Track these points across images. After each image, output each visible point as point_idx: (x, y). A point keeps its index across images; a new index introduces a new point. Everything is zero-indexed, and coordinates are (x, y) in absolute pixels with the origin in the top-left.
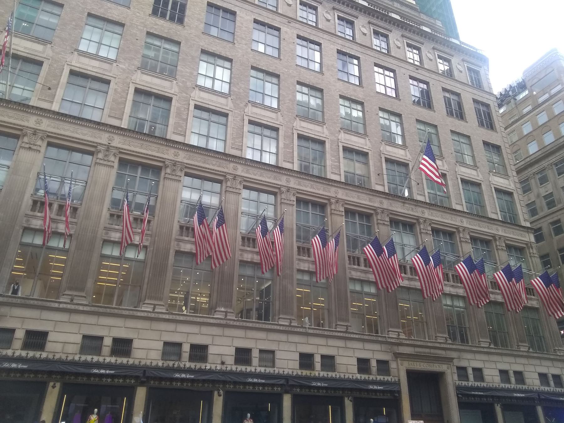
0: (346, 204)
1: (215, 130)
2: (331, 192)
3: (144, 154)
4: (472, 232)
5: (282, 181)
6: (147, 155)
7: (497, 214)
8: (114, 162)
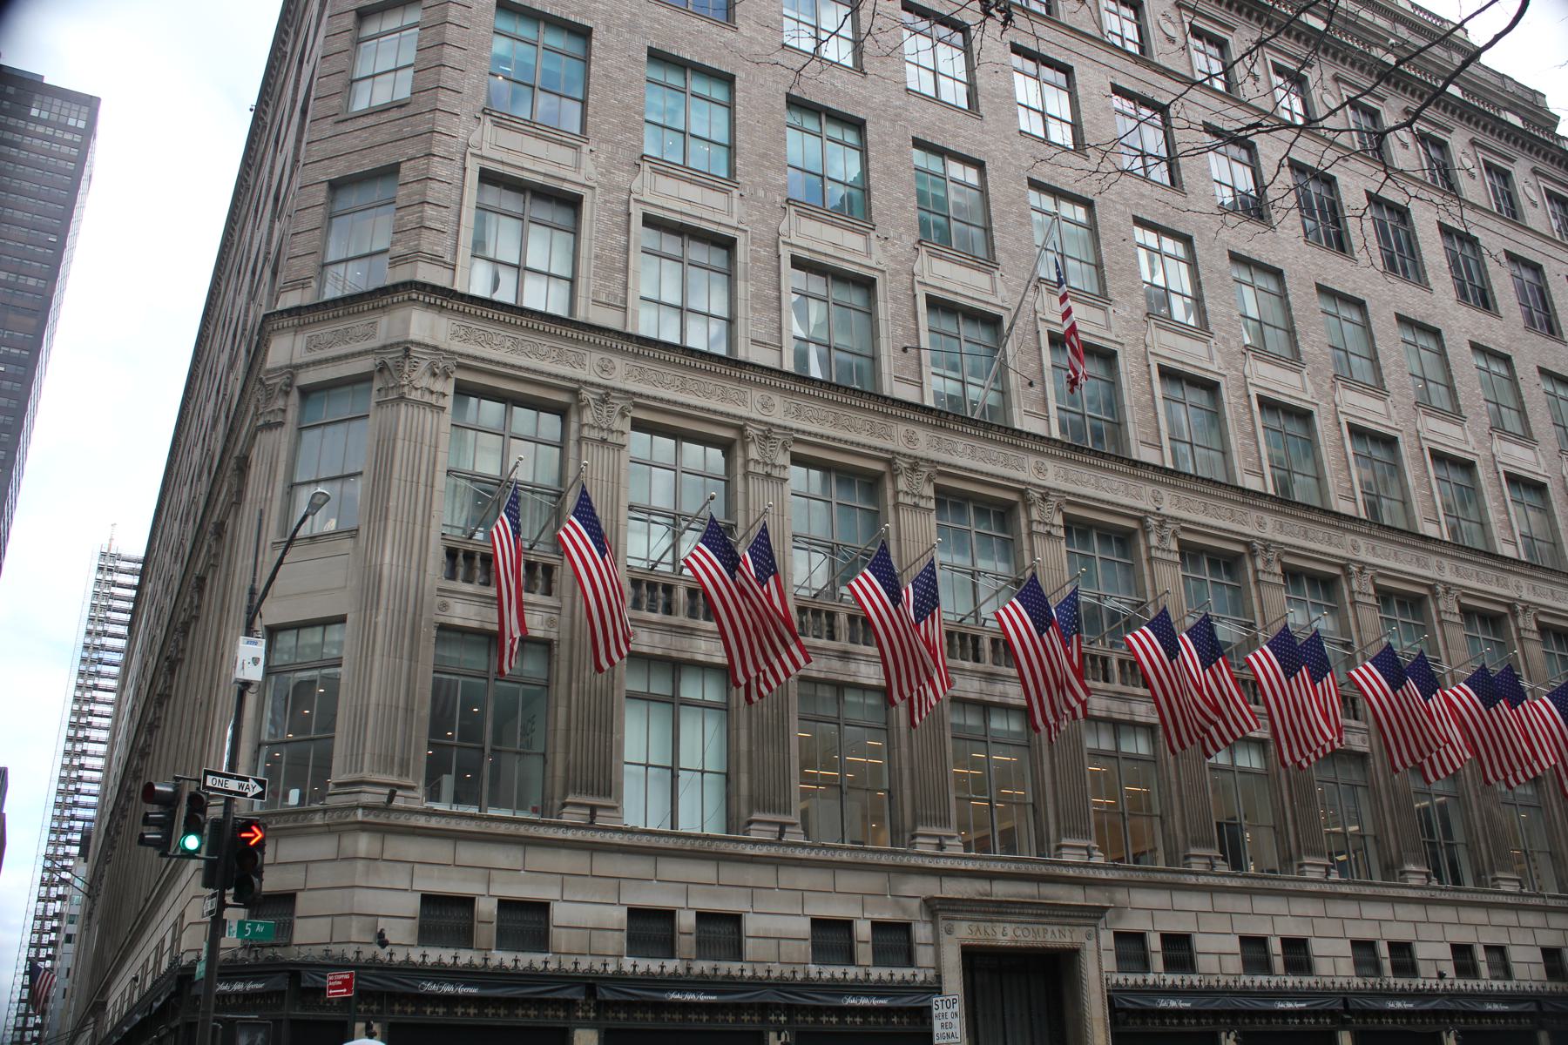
0: (941, 473)
1: (546, 249)
2: (900, 438)
3: (816, 435)
4: (1381, 575)
5: (751, 404)
6: (858, 444)
7: (1439, 523)
8: (444, 395)
